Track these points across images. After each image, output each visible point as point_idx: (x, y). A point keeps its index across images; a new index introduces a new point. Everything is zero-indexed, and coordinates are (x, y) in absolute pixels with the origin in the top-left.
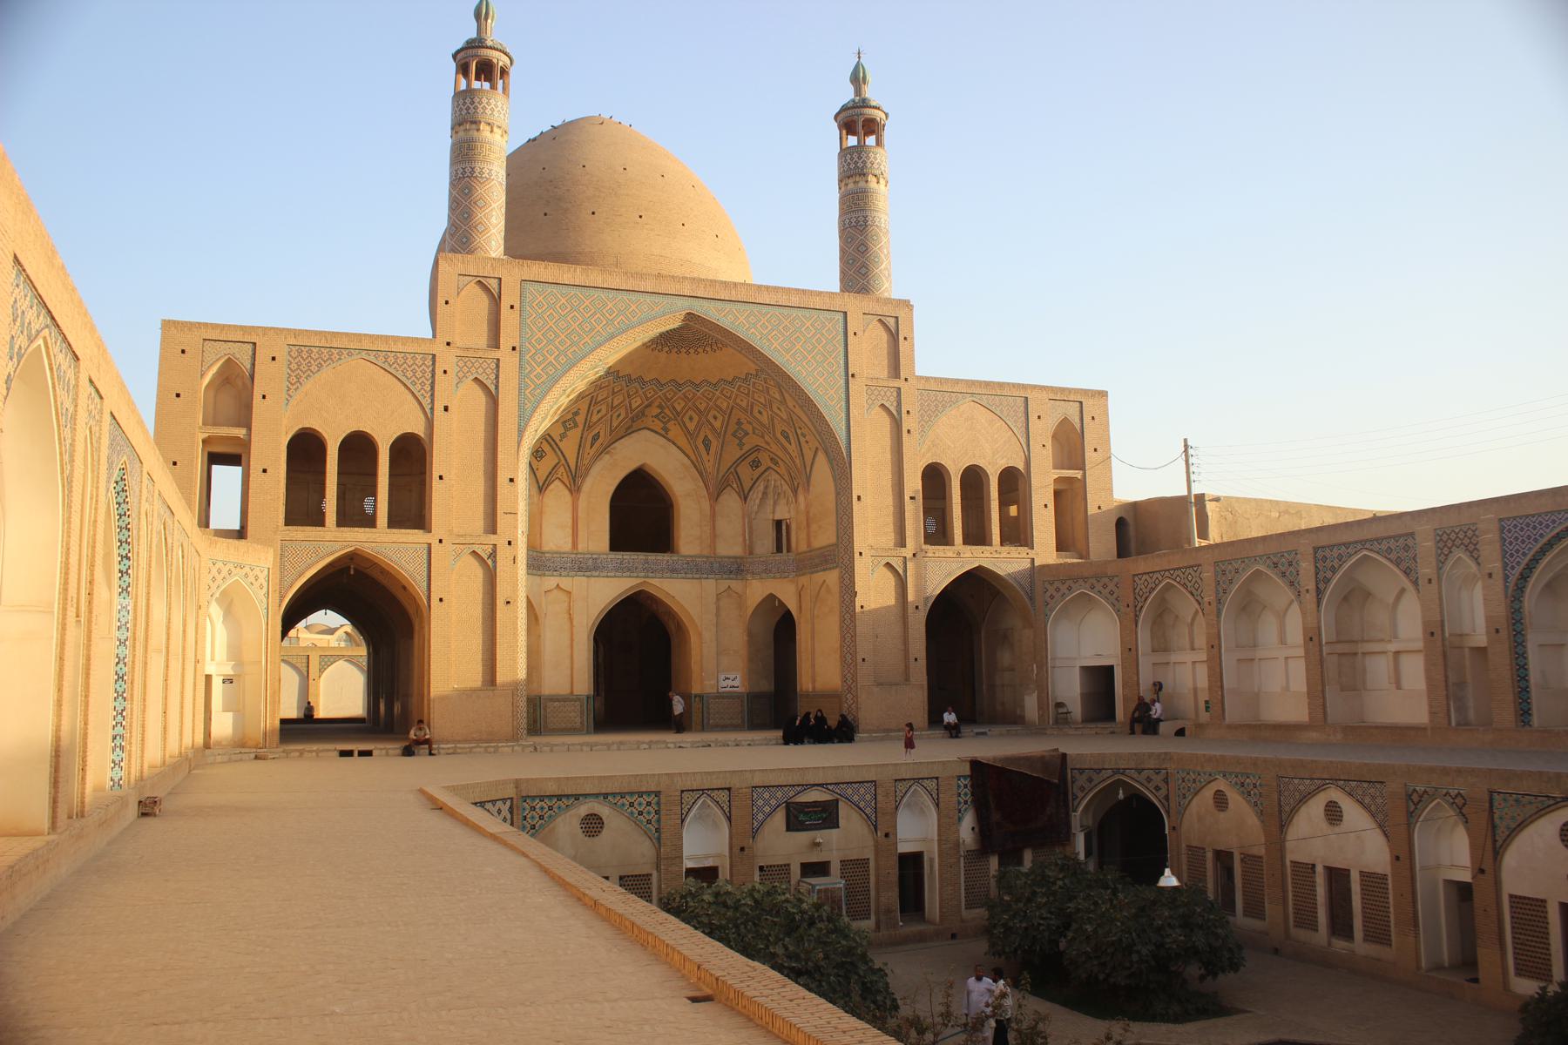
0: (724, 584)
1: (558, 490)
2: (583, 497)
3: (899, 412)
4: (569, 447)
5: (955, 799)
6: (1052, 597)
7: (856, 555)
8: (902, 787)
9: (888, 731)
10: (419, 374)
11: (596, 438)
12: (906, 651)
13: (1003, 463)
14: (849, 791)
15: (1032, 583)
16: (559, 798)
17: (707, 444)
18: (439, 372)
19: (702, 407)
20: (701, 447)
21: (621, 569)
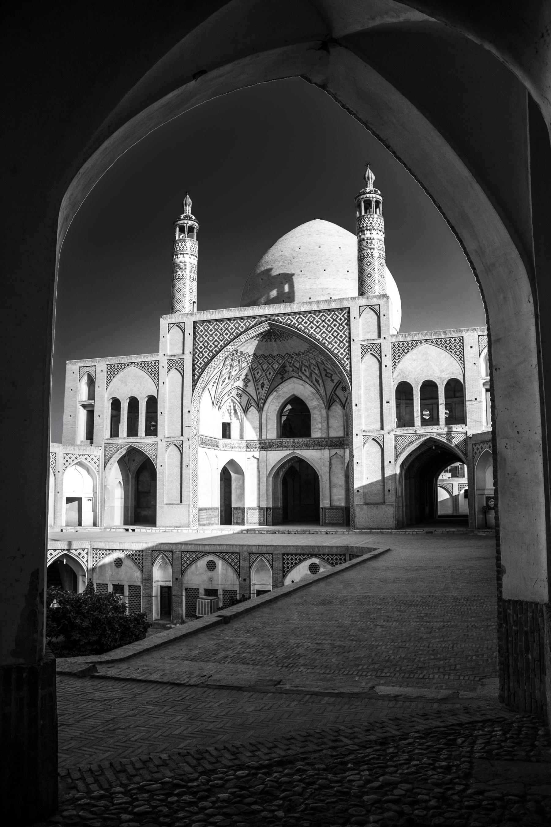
0: (333, 452)
1: (253, 411)
2: (264, 413)
3: (381, 357)
4: (251, 389)
5: (281, 565)
6: (476, 453)
7: (354, 435)
8: (252, 556)
9: (371, 529)
10: (153, 370)
11: (263, 385)
12: (384, 486)
13: (447, 376)
14: (227, 557)
15: (466, 446)
16: (106, 550)
17: (318, 383)
18: (161, 367)
19: (306, 364)
20: (316, 384)
21: (282, 447)
